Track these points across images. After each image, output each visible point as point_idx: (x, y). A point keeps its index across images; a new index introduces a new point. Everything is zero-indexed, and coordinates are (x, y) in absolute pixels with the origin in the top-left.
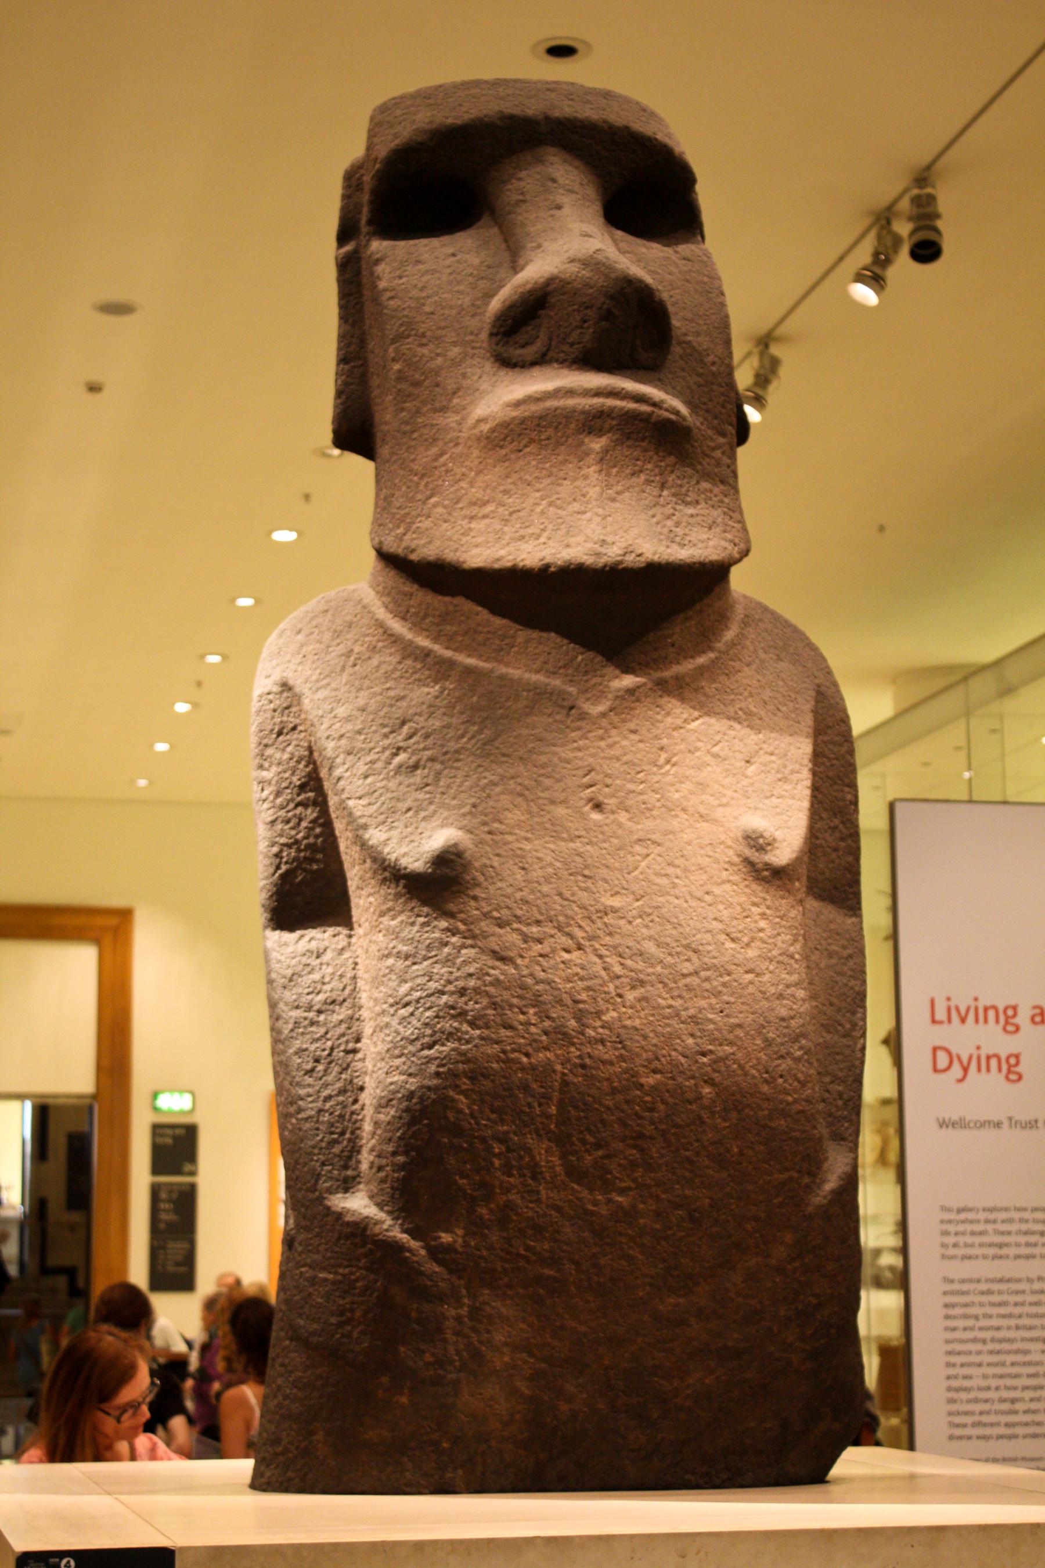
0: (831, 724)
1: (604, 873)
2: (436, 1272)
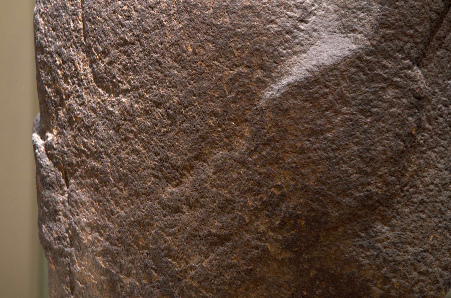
2: (47, 166)
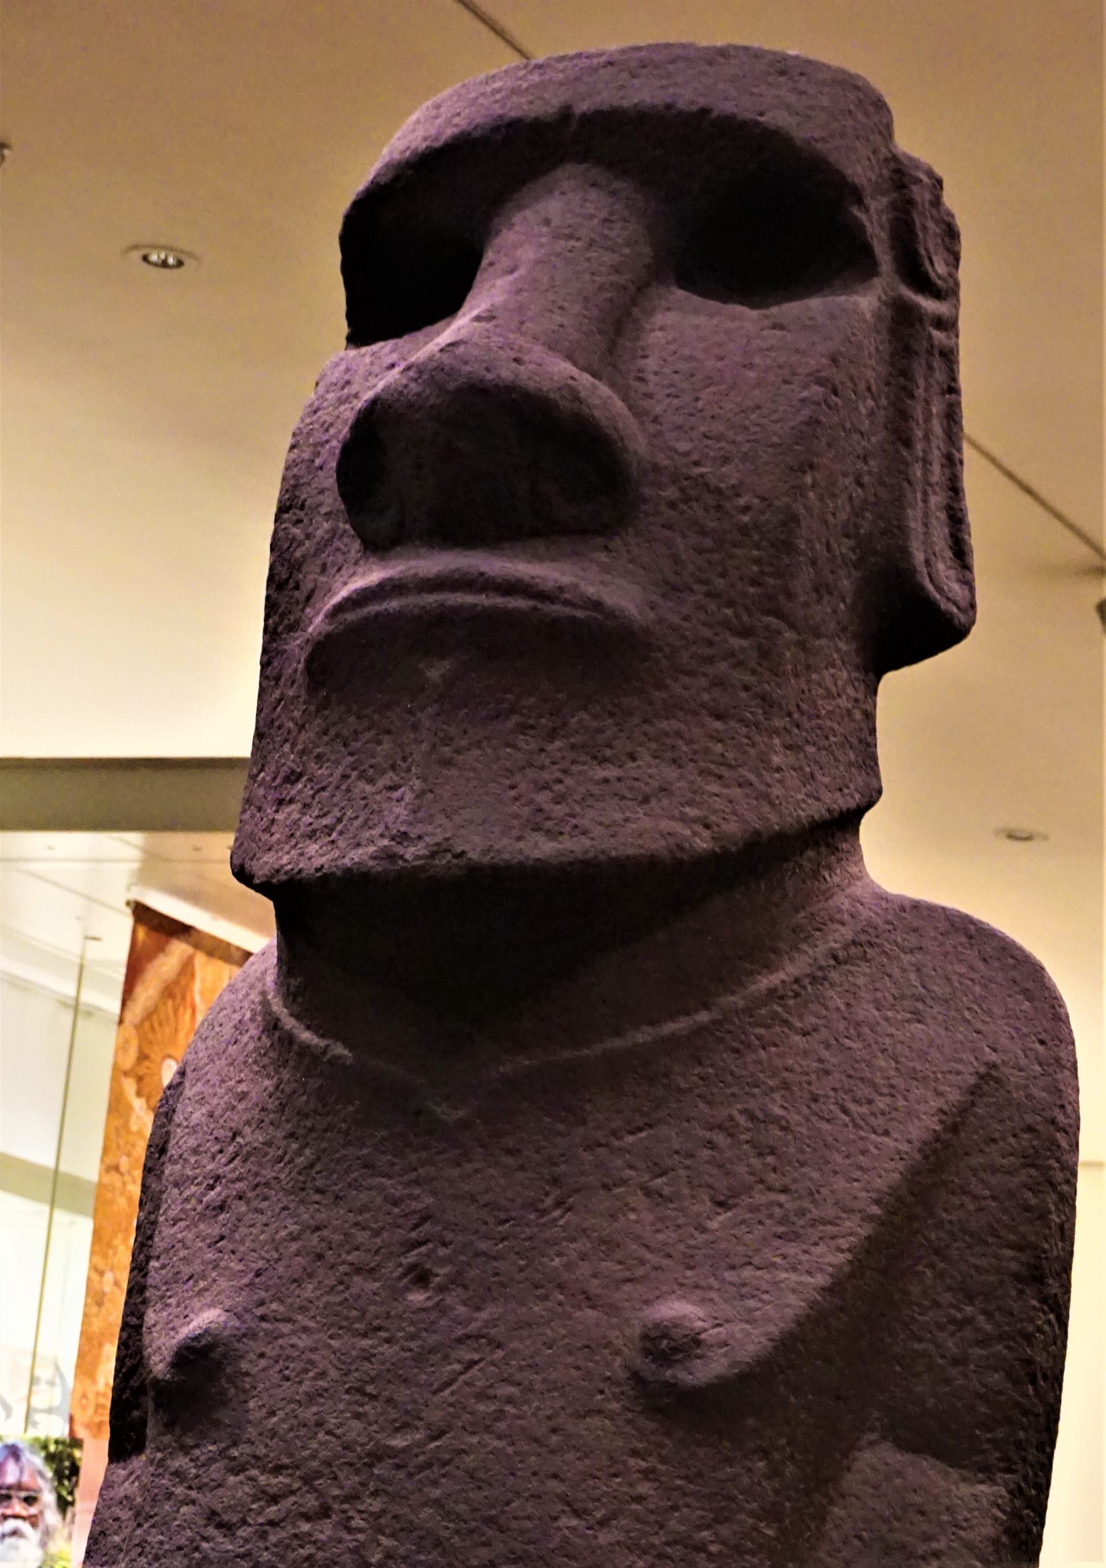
0: (997, 1135)
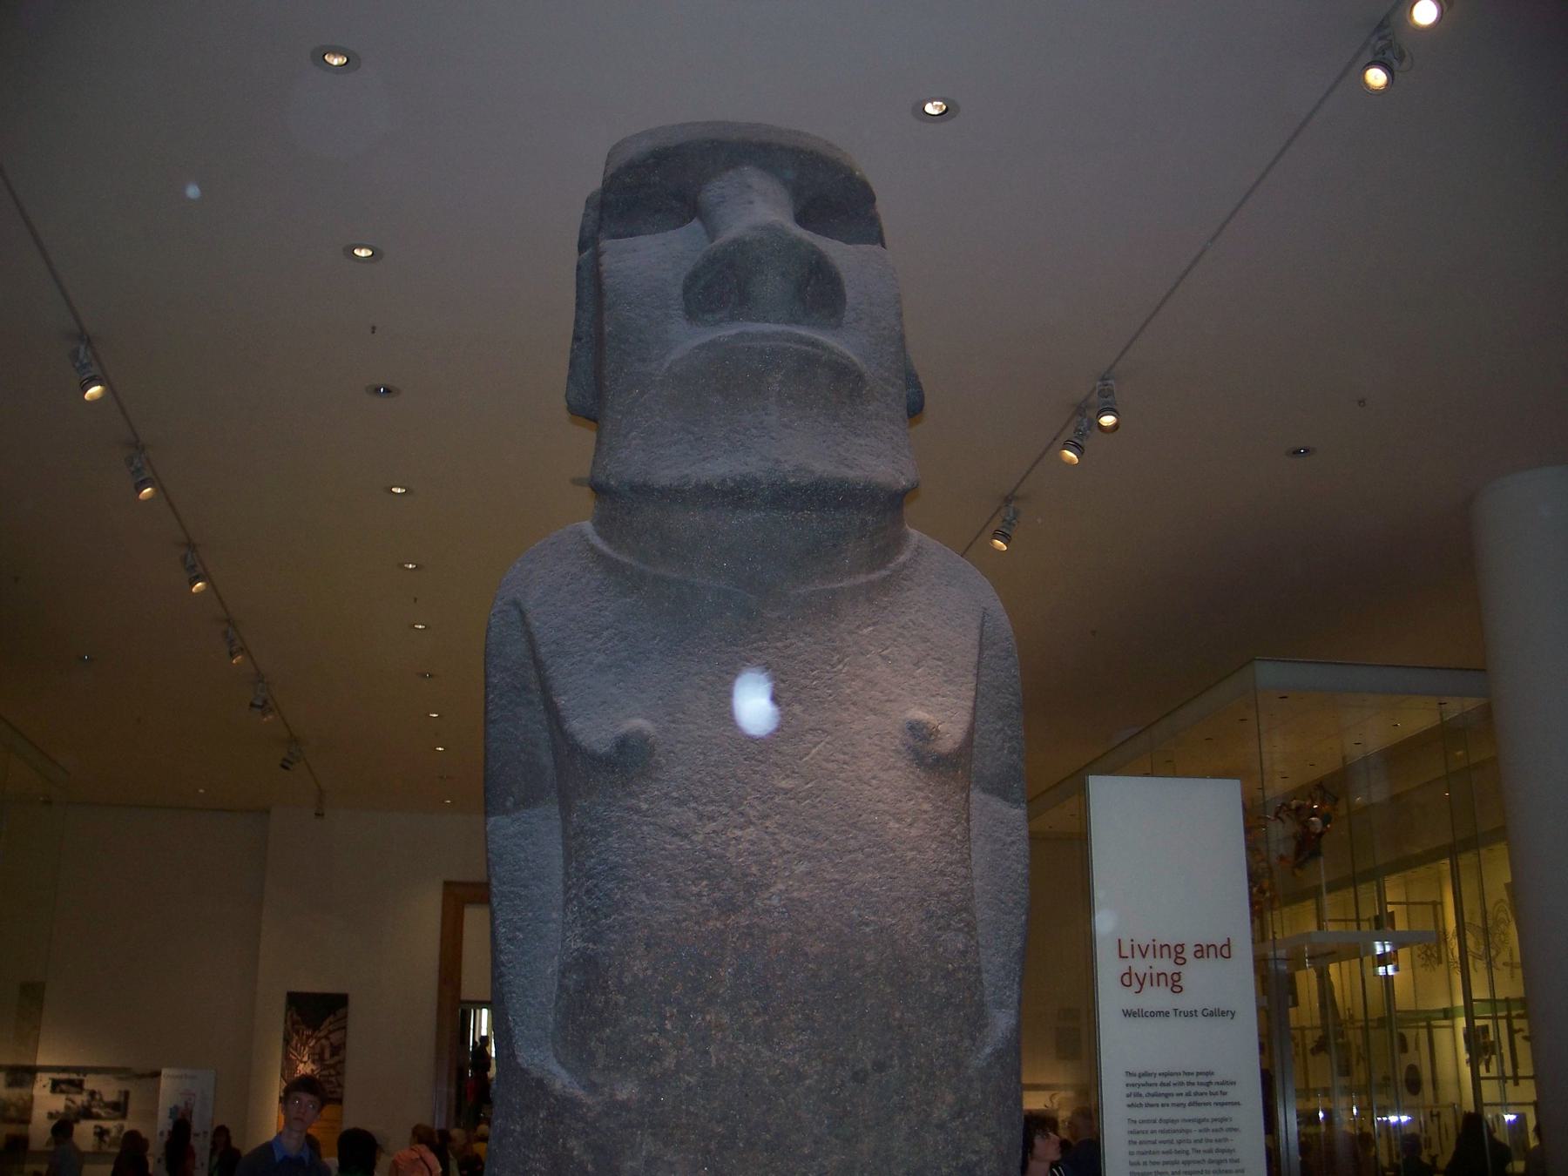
1: (774, 757)
